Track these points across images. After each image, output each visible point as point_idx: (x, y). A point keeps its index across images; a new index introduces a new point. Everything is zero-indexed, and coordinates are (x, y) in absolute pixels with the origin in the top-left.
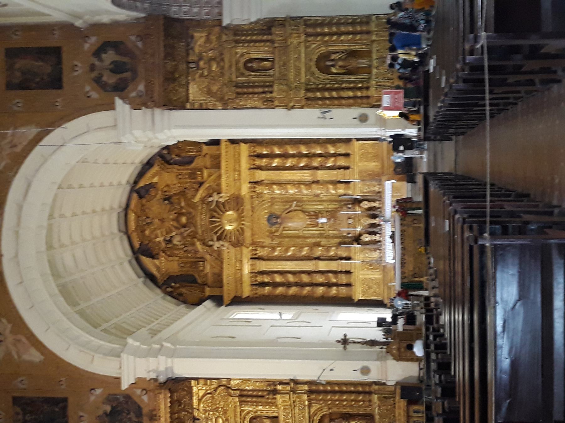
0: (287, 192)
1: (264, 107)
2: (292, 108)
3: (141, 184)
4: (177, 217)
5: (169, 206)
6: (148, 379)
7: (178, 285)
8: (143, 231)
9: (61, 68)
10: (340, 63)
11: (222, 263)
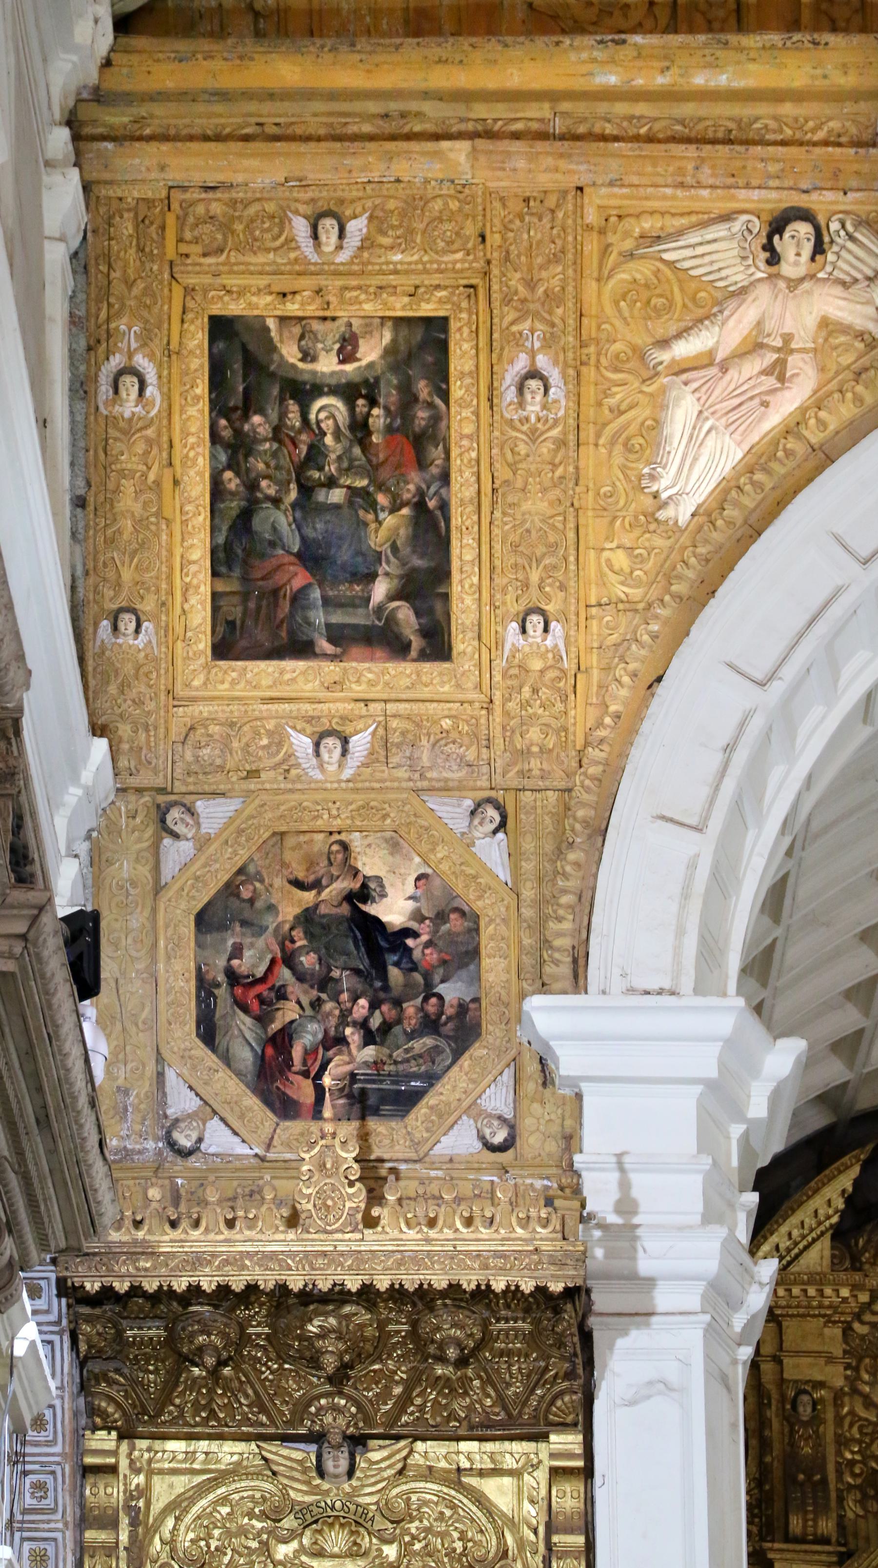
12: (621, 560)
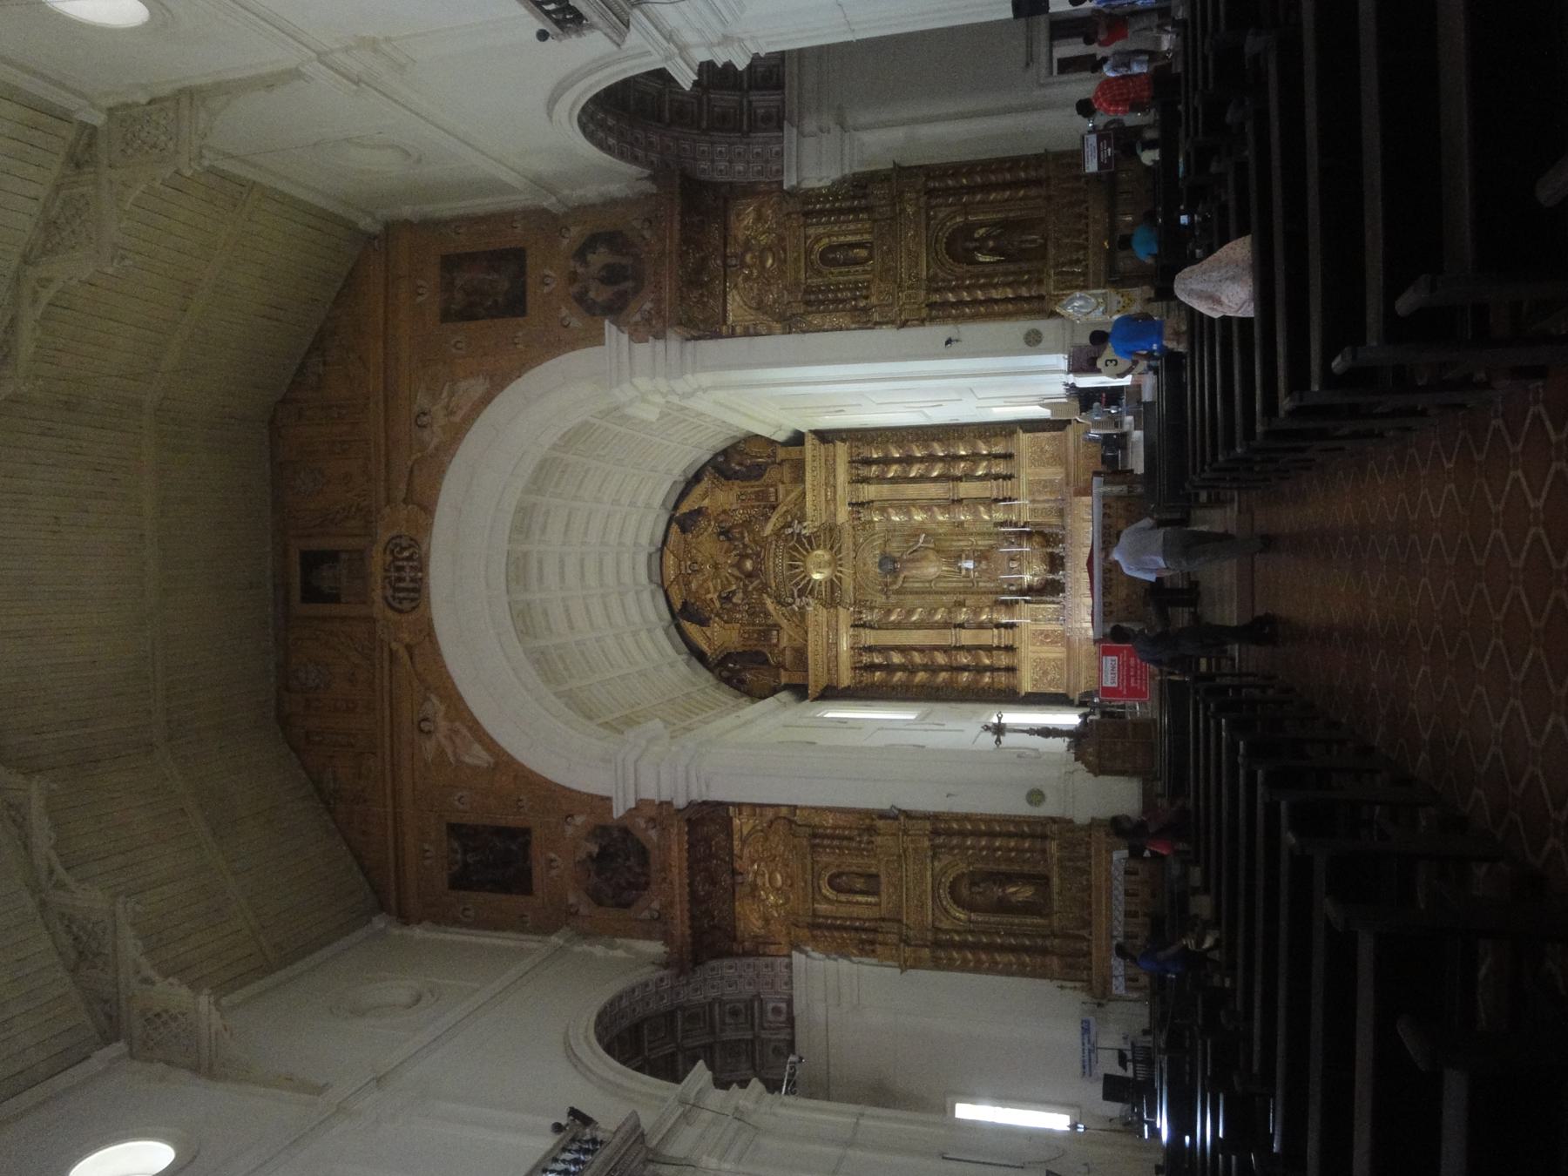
0: (911, 518)
1: (853, 326)
2: (904, 325)
3: (685, 508)
5: (726, 544)
6: (657, 802)
8: (688, 584)
9: (524, 284)
10: (991, 244)
11: (806, 633)
12: (504, 778)
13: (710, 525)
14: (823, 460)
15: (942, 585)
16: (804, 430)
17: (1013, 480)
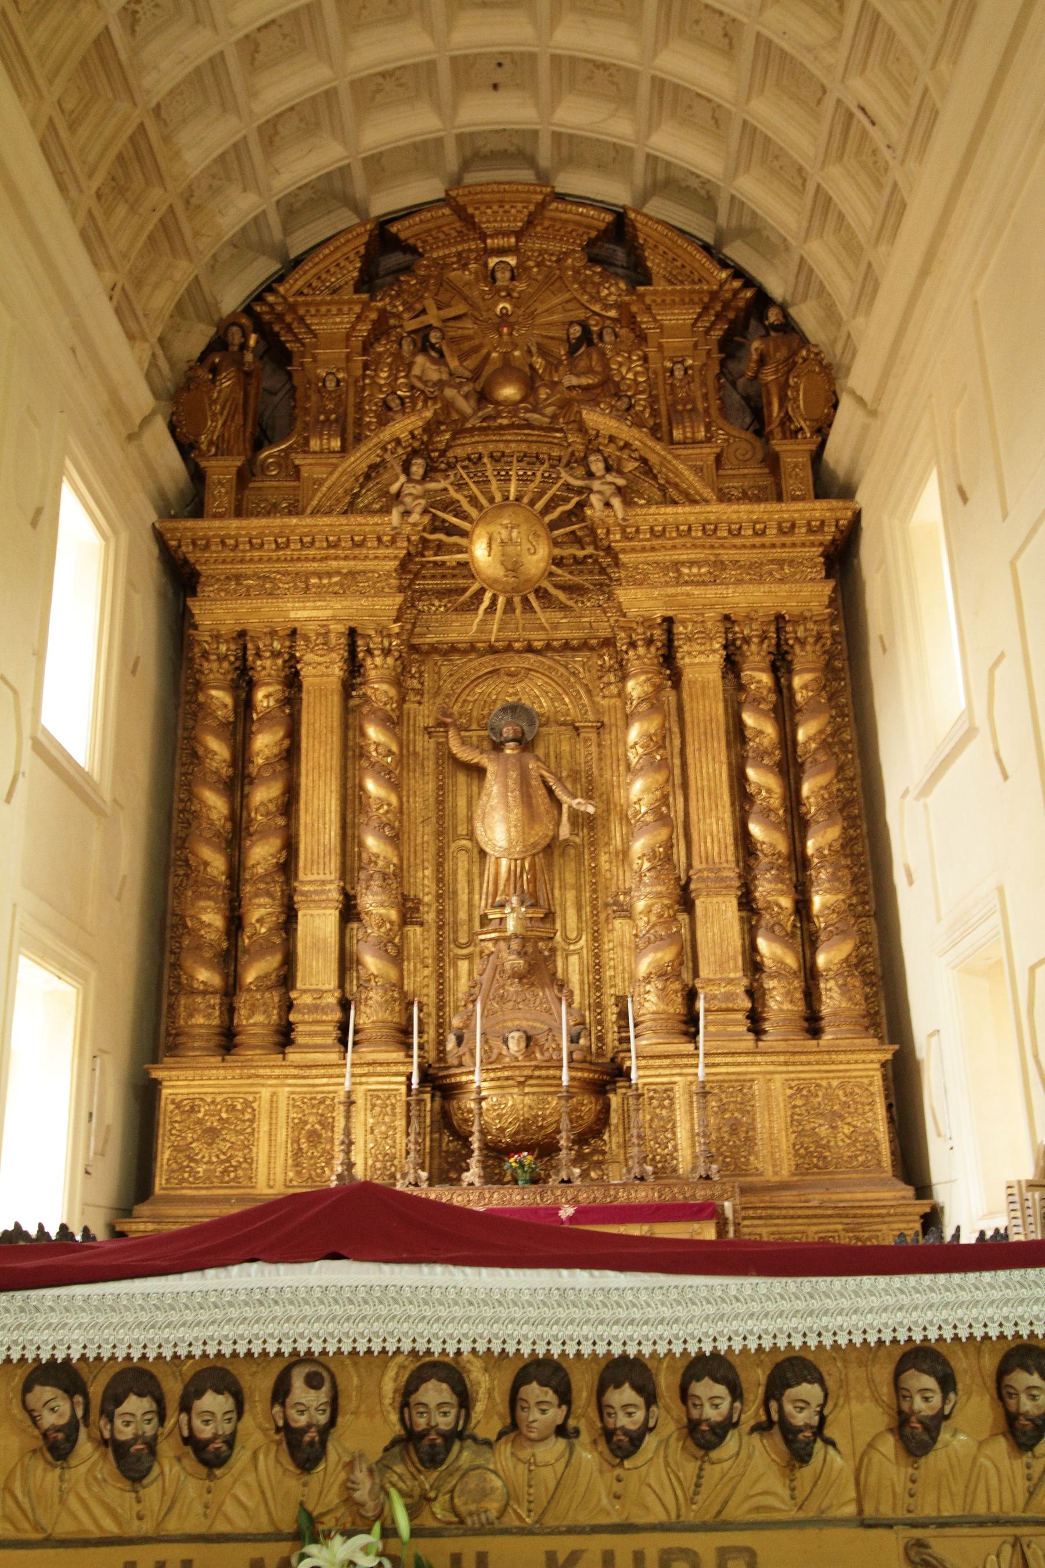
4: (519, 370)
7: (249, 357)
13: (607, 307)
14: (778, 553)
15: (463, 863)
16: (862, 498)
17: (751, 1036)
